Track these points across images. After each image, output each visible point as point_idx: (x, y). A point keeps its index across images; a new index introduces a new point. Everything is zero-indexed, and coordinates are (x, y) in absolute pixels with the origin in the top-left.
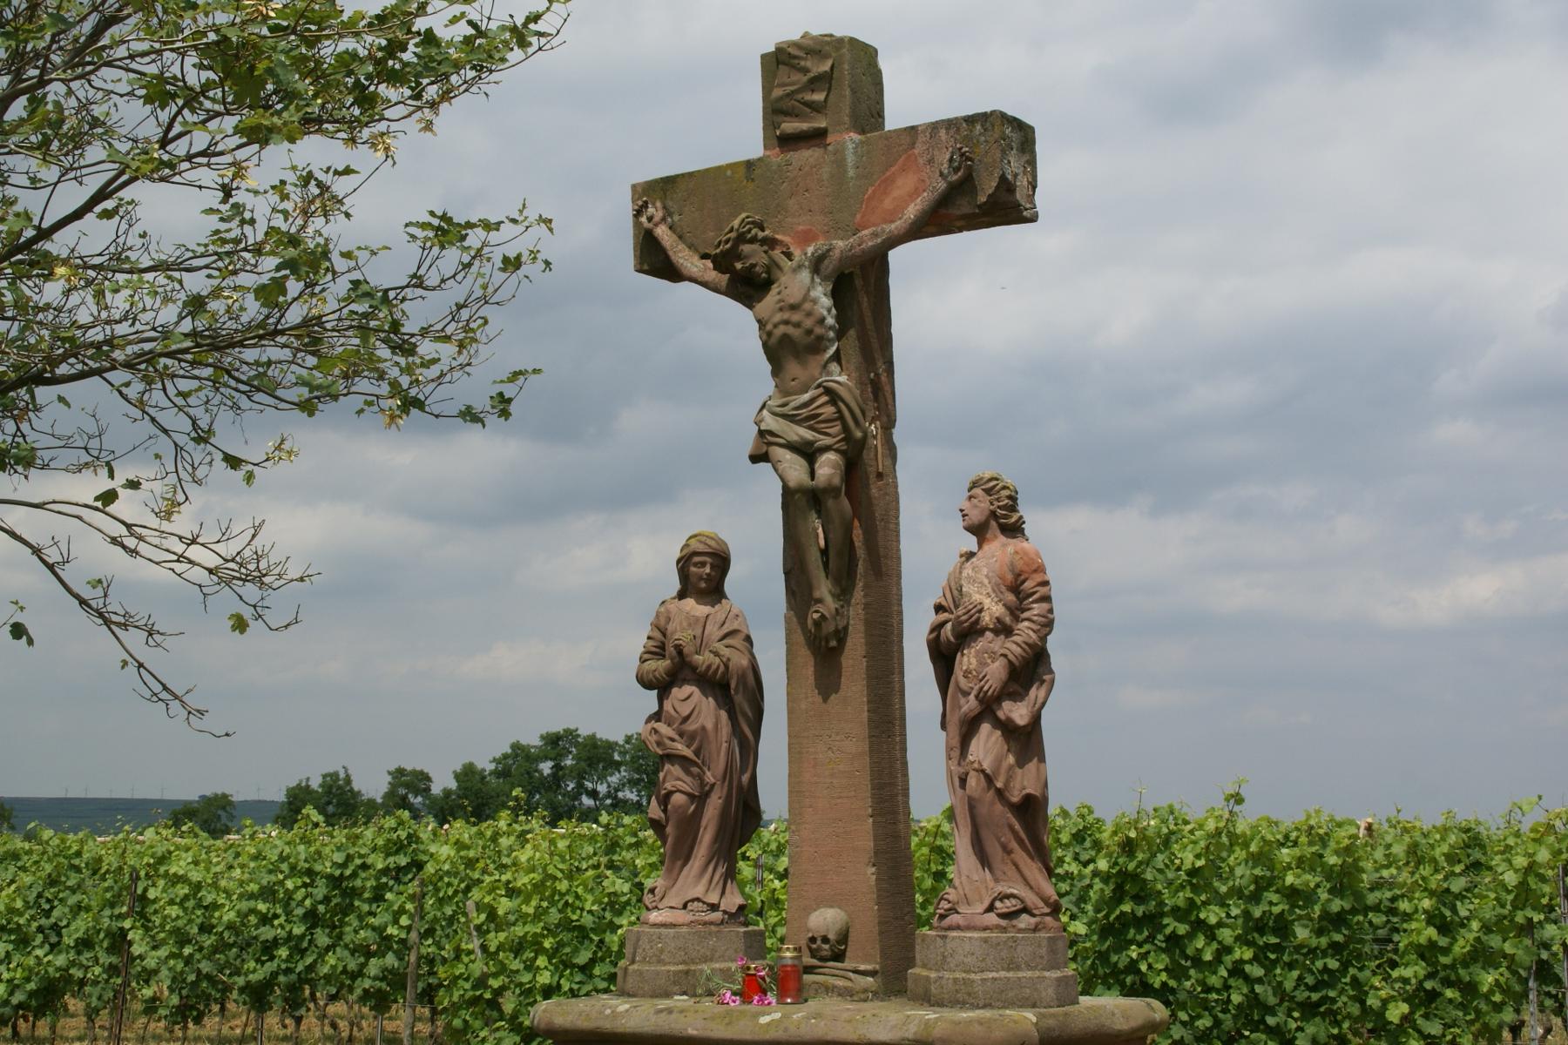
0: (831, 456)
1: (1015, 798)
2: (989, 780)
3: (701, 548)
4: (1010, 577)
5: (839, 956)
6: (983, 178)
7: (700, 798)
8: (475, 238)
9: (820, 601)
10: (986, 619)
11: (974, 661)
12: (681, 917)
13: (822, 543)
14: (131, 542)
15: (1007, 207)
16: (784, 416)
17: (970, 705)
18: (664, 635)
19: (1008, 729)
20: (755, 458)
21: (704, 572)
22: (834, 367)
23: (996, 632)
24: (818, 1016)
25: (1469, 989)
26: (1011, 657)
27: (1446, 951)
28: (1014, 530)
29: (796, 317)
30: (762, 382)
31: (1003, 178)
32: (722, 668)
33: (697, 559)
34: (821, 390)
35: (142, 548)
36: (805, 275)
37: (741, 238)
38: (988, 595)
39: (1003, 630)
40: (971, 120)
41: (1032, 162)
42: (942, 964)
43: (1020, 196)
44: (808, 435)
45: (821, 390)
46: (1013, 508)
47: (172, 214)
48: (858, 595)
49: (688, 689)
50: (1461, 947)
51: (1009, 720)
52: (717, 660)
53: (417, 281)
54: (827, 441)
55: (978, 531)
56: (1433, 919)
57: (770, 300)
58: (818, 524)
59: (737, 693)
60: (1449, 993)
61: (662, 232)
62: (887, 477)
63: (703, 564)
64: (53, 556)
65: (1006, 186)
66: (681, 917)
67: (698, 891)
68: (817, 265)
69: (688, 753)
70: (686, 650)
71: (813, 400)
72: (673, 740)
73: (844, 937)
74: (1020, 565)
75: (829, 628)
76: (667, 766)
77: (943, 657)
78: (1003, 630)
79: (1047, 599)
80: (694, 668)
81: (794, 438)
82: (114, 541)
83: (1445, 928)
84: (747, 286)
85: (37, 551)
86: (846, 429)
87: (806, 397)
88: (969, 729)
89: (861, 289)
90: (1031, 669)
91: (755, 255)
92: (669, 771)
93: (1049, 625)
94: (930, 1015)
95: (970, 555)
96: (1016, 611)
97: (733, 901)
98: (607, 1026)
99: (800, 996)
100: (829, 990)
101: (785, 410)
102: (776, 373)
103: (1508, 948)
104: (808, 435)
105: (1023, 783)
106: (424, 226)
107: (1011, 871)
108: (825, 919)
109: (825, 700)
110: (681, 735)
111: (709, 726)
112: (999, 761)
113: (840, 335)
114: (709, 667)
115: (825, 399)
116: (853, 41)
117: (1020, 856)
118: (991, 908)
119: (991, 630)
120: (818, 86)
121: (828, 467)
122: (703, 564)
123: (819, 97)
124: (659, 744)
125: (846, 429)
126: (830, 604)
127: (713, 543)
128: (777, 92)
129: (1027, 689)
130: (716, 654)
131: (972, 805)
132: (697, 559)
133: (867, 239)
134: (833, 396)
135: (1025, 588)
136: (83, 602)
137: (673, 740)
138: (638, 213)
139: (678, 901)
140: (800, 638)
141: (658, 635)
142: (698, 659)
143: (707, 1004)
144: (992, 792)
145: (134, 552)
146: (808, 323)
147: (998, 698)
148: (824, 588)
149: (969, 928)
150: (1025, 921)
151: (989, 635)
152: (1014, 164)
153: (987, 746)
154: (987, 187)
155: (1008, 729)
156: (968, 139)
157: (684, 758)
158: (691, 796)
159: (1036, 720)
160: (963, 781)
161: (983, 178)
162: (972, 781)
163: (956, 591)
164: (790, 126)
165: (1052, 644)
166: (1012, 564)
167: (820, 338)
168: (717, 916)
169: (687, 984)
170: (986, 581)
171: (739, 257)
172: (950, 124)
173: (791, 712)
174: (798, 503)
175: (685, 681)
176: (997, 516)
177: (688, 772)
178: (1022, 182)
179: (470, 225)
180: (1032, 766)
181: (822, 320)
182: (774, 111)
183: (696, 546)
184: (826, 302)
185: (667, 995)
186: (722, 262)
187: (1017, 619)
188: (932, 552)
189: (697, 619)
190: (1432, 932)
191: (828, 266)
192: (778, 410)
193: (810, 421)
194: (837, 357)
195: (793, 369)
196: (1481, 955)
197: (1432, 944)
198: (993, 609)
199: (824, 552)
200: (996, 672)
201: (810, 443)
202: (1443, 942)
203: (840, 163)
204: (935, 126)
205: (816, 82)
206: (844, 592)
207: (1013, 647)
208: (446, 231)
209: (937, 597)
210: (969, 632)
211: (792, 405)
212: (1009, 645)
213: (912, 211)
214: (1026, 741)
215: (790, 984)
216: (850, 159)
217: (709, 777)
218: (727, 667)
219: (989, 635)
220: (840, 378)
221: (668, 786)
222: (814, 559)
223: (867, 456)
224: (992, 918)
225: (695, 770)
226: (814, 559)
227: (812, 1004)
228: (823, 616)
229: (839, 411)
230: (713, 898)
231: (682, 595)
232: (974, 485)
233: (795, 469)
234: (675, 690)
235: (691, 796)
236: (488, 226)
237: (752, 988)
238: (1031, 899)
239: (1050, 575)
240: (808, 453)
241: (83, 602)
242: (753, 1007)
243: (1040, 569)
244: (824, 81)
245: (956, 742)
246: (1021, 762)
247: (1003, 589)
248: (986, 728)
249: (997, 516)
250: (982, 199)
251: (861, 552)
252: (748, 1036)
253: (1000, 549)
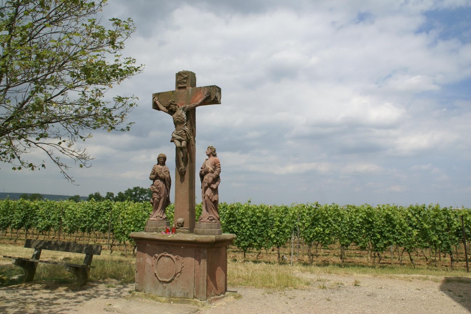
0: (184, 142)
1: (213, 201)
2: (209, 197)
5: (182, 226)
6: (212, 97)
7: (160, 199)
8: (124, 101)
10: (210, 170)
12: (156, 219)
14: (63, 151)
15: (216, 101)
17: (206, 185)
19: (212, 189)
20: (171, 141)
21: (162, 160)
22: (186, 126)
23: (211, 173)
24: (178, 236)
25: (284, 232)
27: (281, 226)
28: (215, 156)
29: (179, 118)
30: (173, 128)
31: (215, 96)
35: (65, 152)
36: (181, 111)
37: (171, 104)
39: (212, 172)
40: (210, 86)
41: (220, 94)
42: (200, 228)
43: (218, 100)
44: (181, 138)
46: (215, 152)
47: (74, 95)
48: (188, 165)
49: (158, 180)
50: (283, 226)
53: (115, 108)
55: (209, 155)
56: (279, 221)
57: (175, 114)
59: (167, 181)
60: (281, 233)
61: (157, 102)
62: (194, 146)
64: (50, 153)
65: (216, 98)
66: (156, 219)
67: (159, 215)
68: (183, 109)
69: (158, 191)
73: (183, 223)
74: (215, 161)
75: (183, 171)
77: (202, 176)
78: (212, 172)
79: (220, 167)
80: (159, 177)
82: (60, 151)
83: (281, 223)
84: (171, 112)
85: (47, 152)
86: (187, 137)
88: (206, 189)
89: (191, 113)
90: (217, 179)
91: (173, 107)
93: (220, 172)
94: (197, 236)
95: (207, 159)
96: (215, 169)
97: (165, 216)
98: (142, 237)
99: (175, 233)
100: (180, 232)
102: (175, 127)
103: (290, 226)
104: (181, 138)
105: (215, 198)
106: (116, 98)
107: (212, 213)
108: (180, 220)
112: (210, 194)
113: (187, 121)
116: (191, 72)
117: (213, 210)
118: (208, 219)
120: (185, 79)
121: (184, 143)
123: (185, 81)
125: (187, 137)
126: (183, 167)
128: (178, 80)
129: (216, 182)
131: (206, 202)
133: (192, 105)
134: (185, 131)
135: (216, 165)
136: (55, 161)
138: (153, 99)
139: (155, 216)
143: (160, 233)
145: (64, 153)
146: (182, 119)
148: (182, 164)
149: (204, 222)
150: (214, 221)
152: (217, 94)
153: (209, 192)
154: (213, 98)
155: (212, 189)
156: (210, 90)
159: (217, 188)
160: (204, 198)
161: (212, 97)
162: (206, 198)
163: (205, 166)
164: (180, 85)
165: (220, 175)
167: (183, 121)
168: (162, 219)
169: (156, 230)
171: (170, 107)
172: (207, 87)
173: (176, 185)
174: (178, 149)
176: (212, 153)
178: (219, 97)
179: (124, 98)
180: (216, 195)
181: (184, 118)
182: (178, 83)
183: (160, 156)
184: (185, 115)
185: (153, 232)
186: (167, 108)
187: (215, 171)
188: (201, 159)
190: (279, 223)
191: (185, 109)
193: (181, 135)
194: (186, 125)
195: (179, 126)
196: (286, 227)
197: (279, 225)
198: (211, 169)
199: (183, 158)
200: (211, 179)
202: (280, 225)
203: (188, 92)
204: (204, 87)
205: (185, 79)
206: (186, 165)
207: (214, 175)
208: (120, 99)
209: (201, 166)
210: (206, 172)
213: (200, 101)
214: (215, 191)
215: (174, 231)
216: (190, 92)
217: (161, 195)
220: (187, 128)
222: (181, 159)
223: (190, 142)
224: (208, 220)
226: (181, 159)
227: (177, 234)
230: (161, 216)
231: (158, 164)
232: (208, 148)
233: (178, 143)
236: (127, 98)
237: (167, 231)
238: (215, 217)
239: (220, 163)
240: (181, 141)
241: (55, 161)
242: (168, 234)
243: (219, 162)
244: (186, 78)
245: (203, 191)
246: (214, 195)
248: (209, 189)
249: (212, 153)
250: (212, 100)
251: (189, 158)
252: (166, 239)
253: (212, 159)
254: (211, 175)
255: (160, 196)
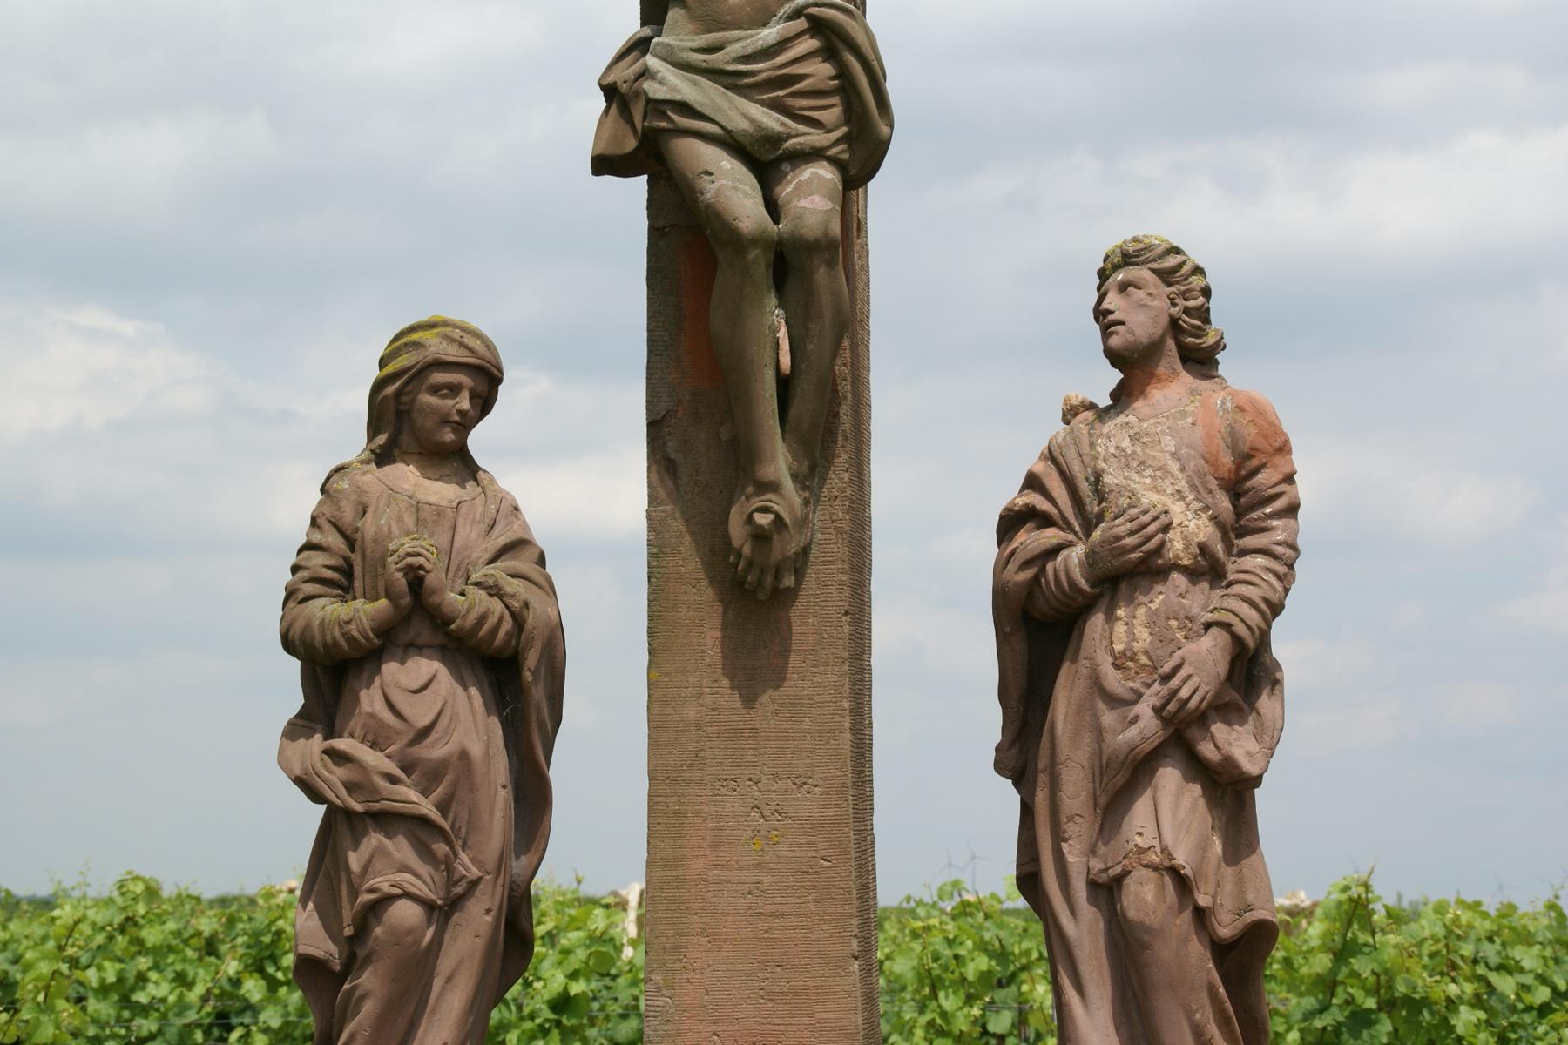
1: (1226, 929)
3: (453, 353)
4: (1227, 460)
7: (442, 911)
9: (773, 487)
10: (1176, 546)
11: (1143, 635)
13: (786, 361)
16: (713, 74)
18: (352, 544)
21: (429, 403)
23: (1193, 574)
26: (1240, 629)
32: (508, 624)
33: (440, 377)
34: (801, 24)
38: (1180, 495)
39: (1208, 570)
44: (772, 121)
45: (801, 24)
46: (1204, 314)
49: (424, 667)
51: (1229, 762)
52: (497, 606)
54: (816, 138)
58: (777, 317)
59: (515, 673)
63: (454, 390)
69: (426, 807)
70: (431, 580)
71: (782, 44)
72: (394, 780)
74: (1250, 434)
76: (374, 839)
78: (1208, 570)
80: (439, 620)
81: (739, 124)
87: (769, 34)
92: (380, 851)
96: (1235, 529)
101: (717, 59)
104: (772, 121)
109: (750, 701)
110: (408, 768)
111: (476, 750)
114: (483, 618)
115: (809, 44)
119: (1185, 570)
122: (454, 390)
124: (351, 787)
127: (477, 344)
130: (495, 591)
132: (440, 377)
137: (394, 780)
140: (688, 561)
141: (332, 539)
142: (452, 599)
144: (1187, 915)
147: (1202, 718)
151: (1177, 578)
157: (423, 820)
158: (429, 906)
166: (1233, 433)
170: (1174, 466)
173: (656, 725)
175: (413, 648)
177: (426, 853)
183: (436, 346)
189: (439, 512)
192: (699, 58)
193: (775, 87)
198: (1191, 527)
199: (785, 385)
201: (775, 140)
210: (1128, 573)
211: (736, 49)
212: (1233, 603)
217: (466, 866)
218: (519, 620)
219: (1177, 578)
221: (383, 883)
225: (441, 848)
228: (778, 519)
229: (843, 74)
231: (382, 457)
234: (390, 668)
235: (429, 906)
243: (1284, 449)
247: (1213, 484)
248: (1169, 777)
249: (1161, 327)
254: (1199, 600)
255: (446, 866)
